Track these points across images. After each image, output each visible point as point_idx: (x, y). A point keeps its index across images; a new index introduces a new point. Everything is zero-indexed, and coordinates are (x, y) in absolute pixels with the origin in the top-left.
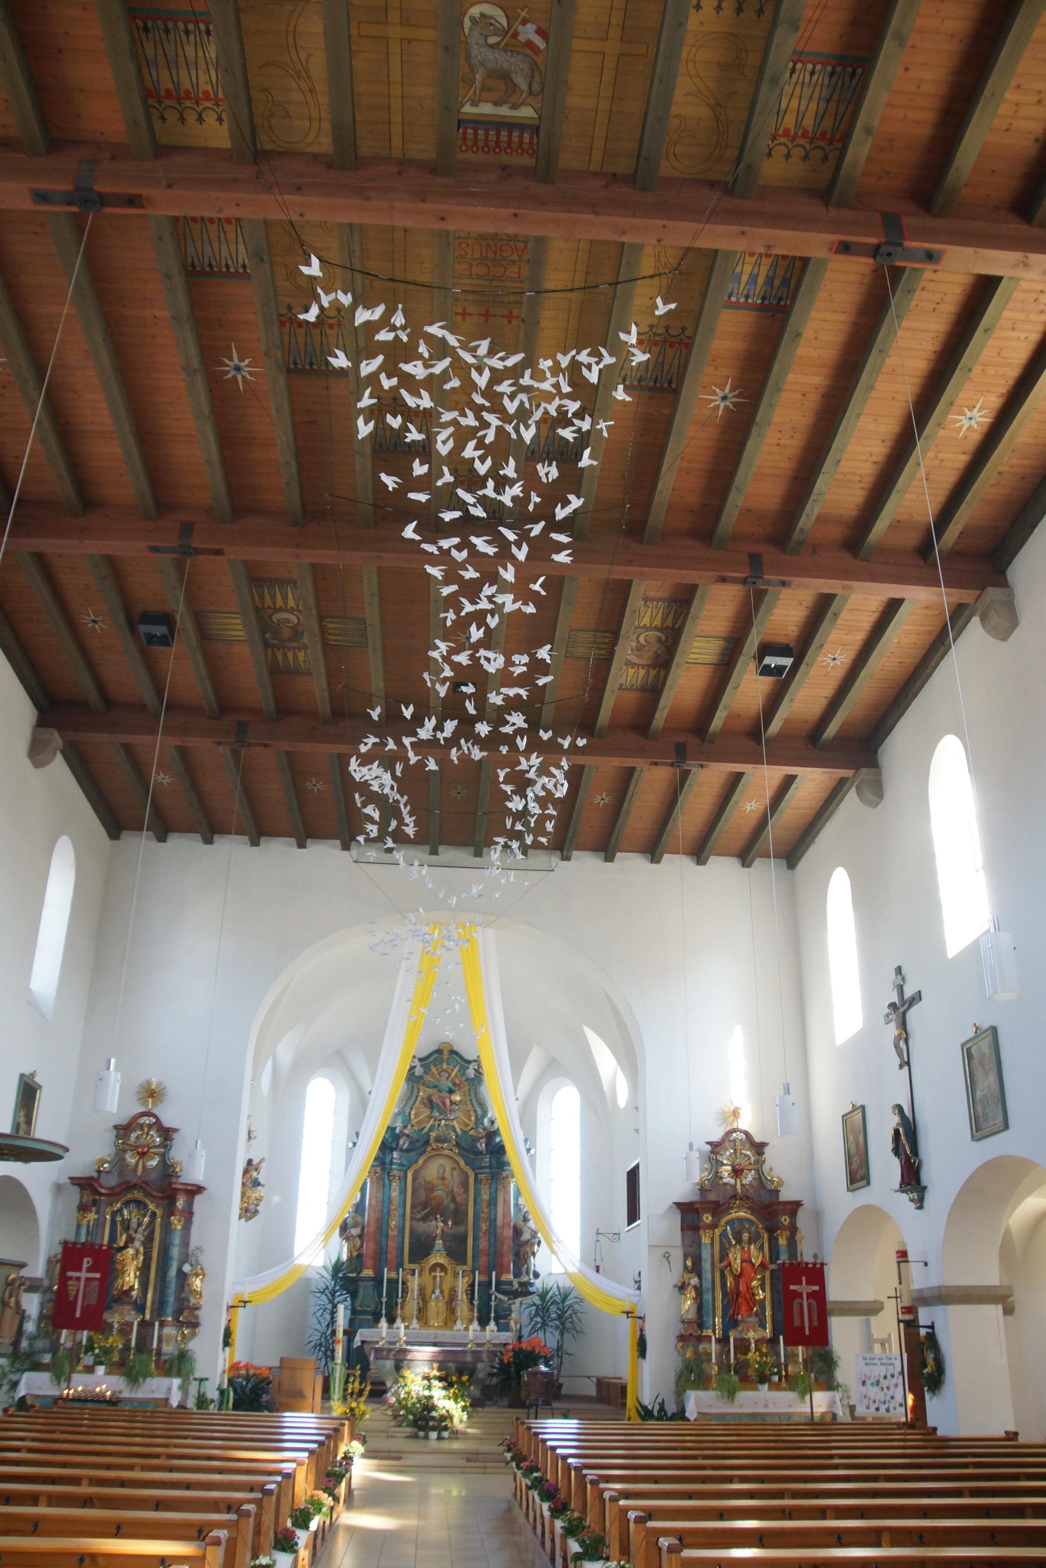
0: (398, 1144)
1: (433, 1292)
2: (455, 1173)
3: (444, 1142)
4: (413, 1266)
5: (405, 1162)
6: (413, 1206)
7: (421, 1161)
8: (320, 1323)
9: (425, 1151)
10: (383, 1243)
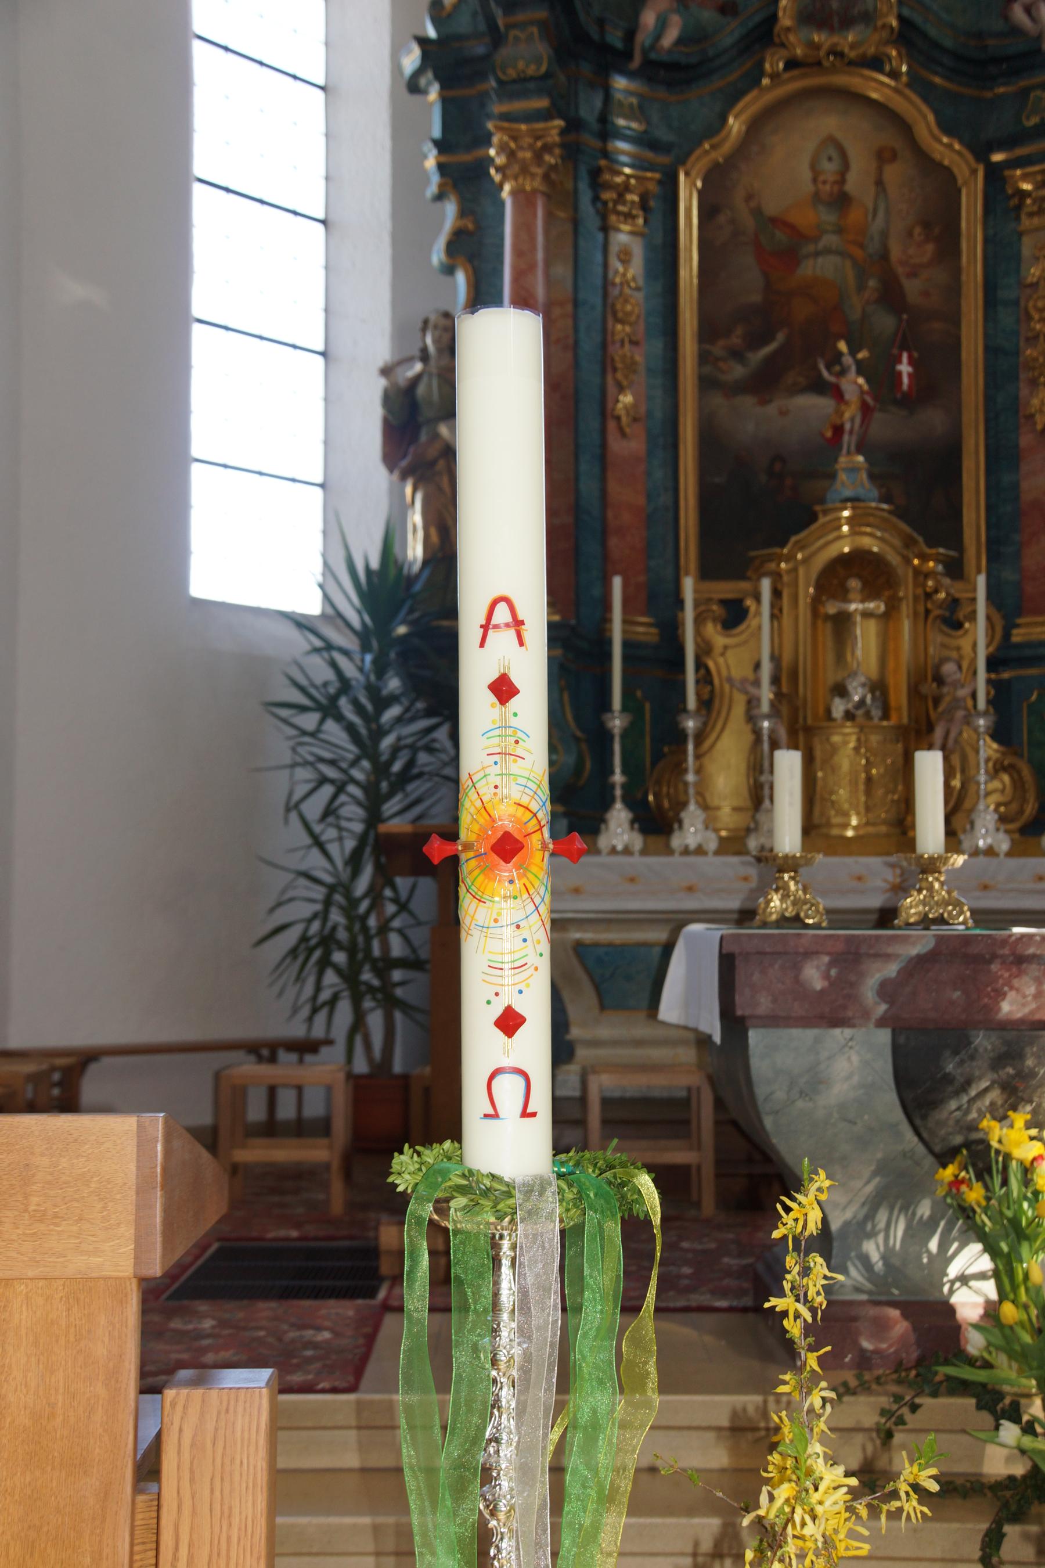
0: (630, 35)
1: (841, 691)
2: (892, 173)
3: (847, 22)
4: (727, 589)
5: (663, 134)
6: (708, 332)
7: (735, 124)
8: (318, 843)
9: (753, 79)
10: (589, 487)
